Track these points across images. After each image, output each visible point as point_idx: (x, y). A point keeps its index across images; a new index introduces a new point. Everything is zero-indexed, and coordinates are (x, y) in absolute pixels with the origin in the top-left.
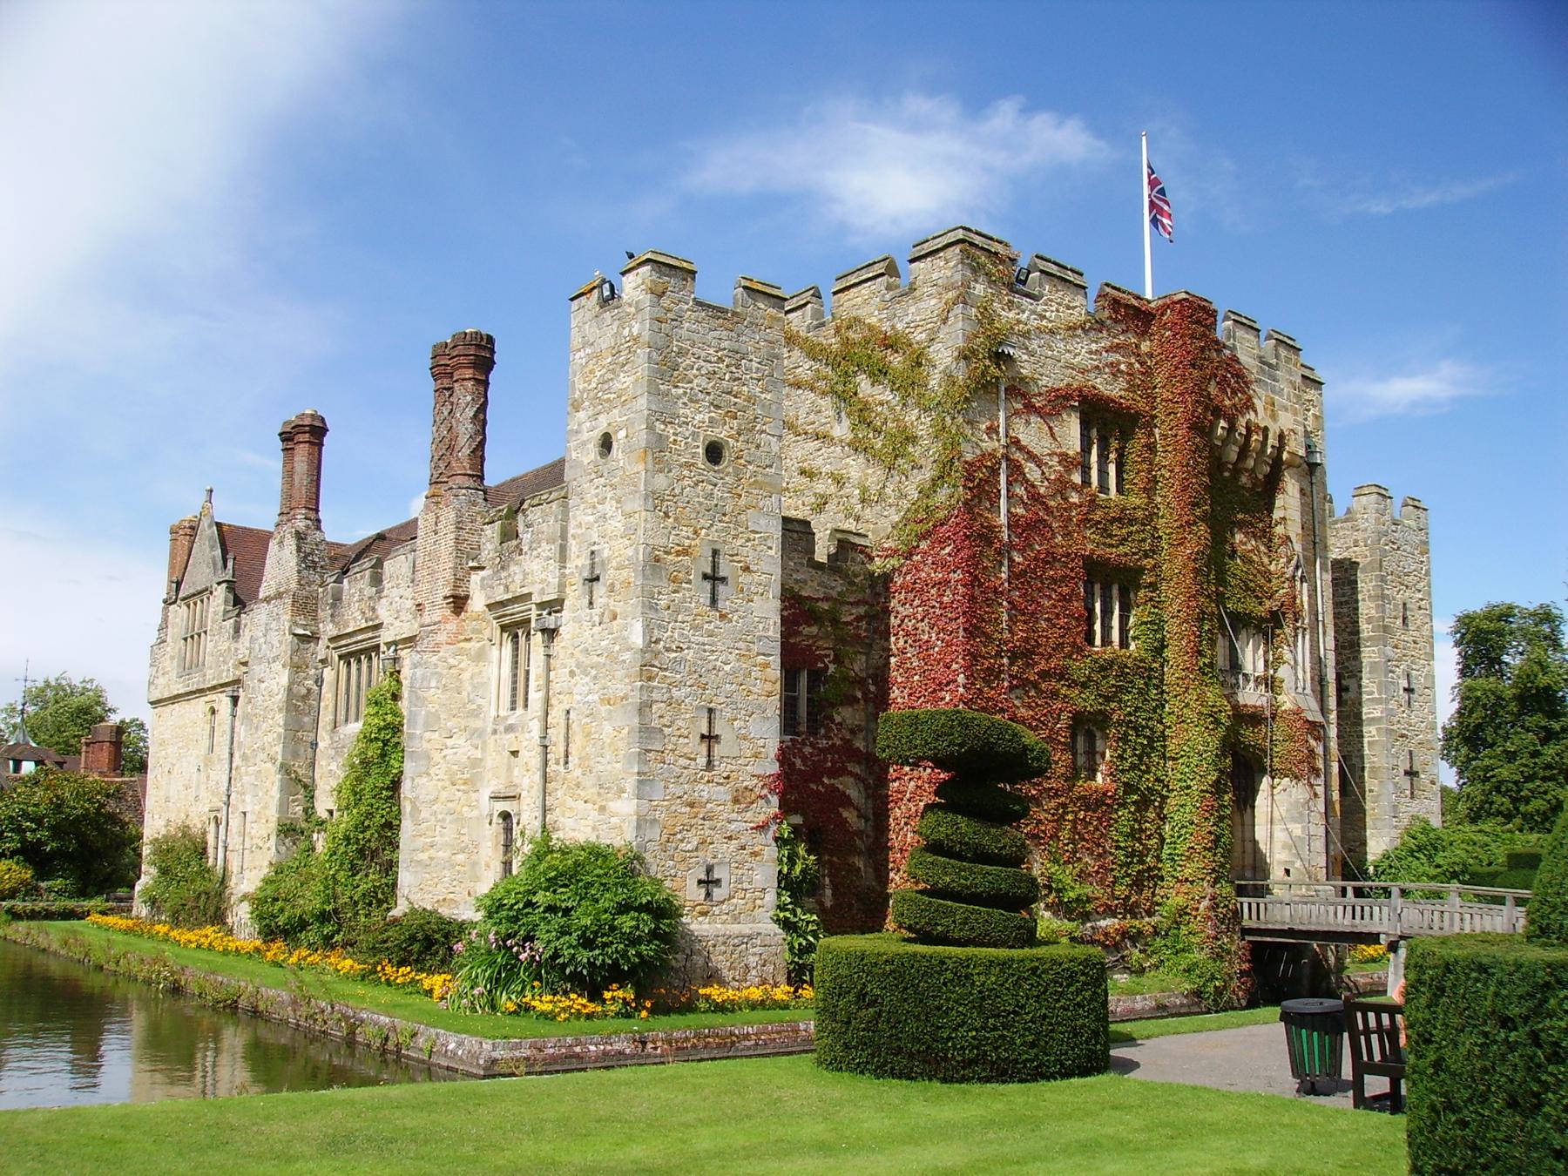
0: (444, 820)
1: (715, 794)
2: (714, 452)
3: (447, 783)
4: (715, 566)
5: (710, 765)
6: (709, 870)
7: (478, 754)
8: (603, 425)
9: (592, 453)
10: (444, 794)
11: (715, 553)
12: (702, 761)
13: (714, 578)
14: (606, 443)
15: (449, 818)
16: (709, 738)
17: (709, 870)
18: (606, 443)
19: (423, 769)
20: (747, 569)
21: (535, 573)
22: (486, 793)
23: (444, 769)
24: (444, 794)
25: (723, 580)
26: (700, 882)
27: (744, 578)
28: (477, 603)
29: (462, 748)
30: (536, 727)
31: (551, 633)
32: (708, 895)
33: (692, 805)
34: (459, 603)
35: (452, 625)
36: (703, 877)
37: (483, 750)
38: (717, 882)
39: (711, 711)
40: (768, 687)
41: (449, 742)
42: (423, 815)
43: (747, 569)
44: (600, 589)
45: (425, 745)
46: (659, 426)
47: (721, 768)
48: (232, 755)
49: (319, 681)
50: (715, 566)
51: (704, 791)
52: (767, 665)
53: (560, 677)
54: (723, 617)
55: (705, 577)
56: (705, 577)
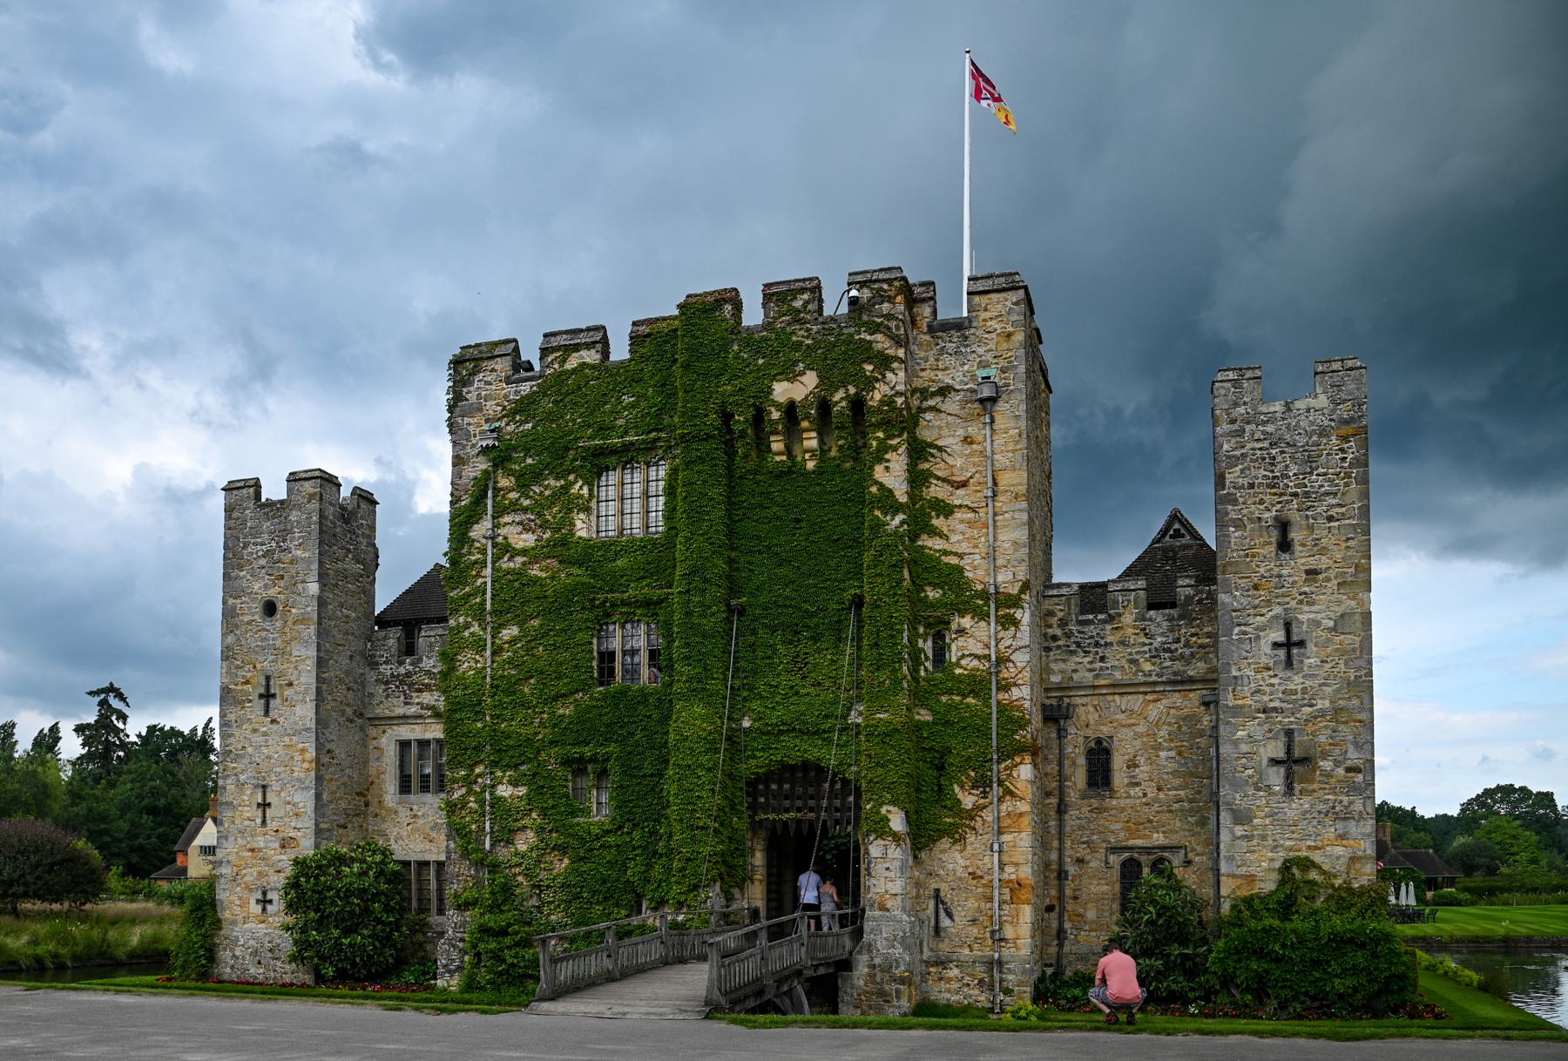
1: (267, 842)
4: (268, 687)
5: (264, 822)
6: (264, 893)
11: (268, 678)
12: (259, 821)
13: (267, 696)
16: (265, 805)
17: (264, 893)
20: (290, 684)
25: (274, 696)
26: (258, 901)
27: (288, 692)
32: (264, 909)
33: (252, 850)
36: (260, 897)
38: (270, 902)
39: (264, 787)
40: (306, 765)
43: (290, 684)
46: (231, 601)
47: (272, 825)
50: (268, 687)
51: (260, 842)
52: (303, 750)
54: (273, 721)
55: (261, 696)
56: (261, 696)
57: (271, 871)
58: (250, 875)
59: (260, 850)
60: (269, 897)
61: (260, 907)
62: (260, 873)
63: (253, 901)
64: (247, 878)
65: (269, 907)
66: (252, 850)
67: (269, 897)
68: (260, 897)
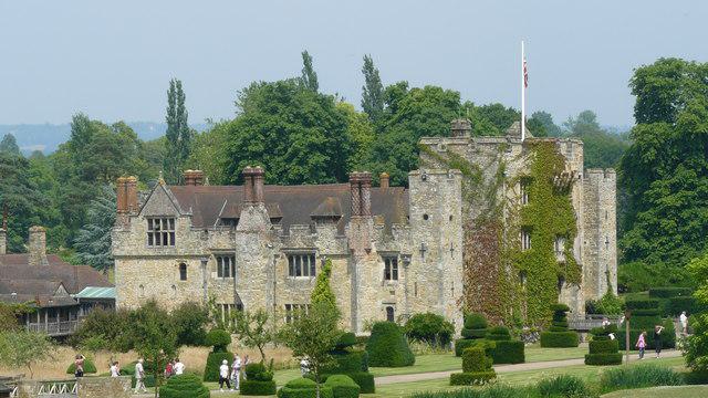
2: (451, 218)
8: (424, 212)
9: (420, 219)
14: (426, 217)
18: (426, 217)
21: (400, 246)
22: (379, 303)
28: (374, 250)
29: (372, 290)
30: (402, 287)
31: (407, 264)
34: (368, 251)
35: (367, 257)
44: (426, 255)
48: (205, 282)
49: (275, 262)
53: (411, 274)
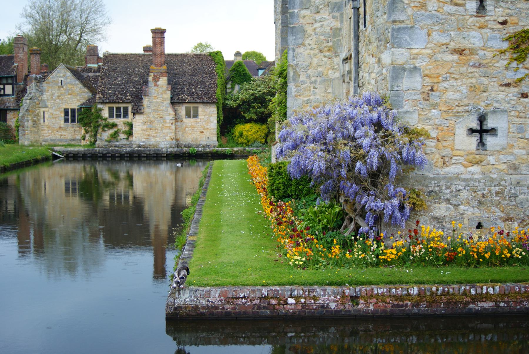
0: (315, 82)
3: (317, 51)
6: (482, 119)
7: (337, 24)
10: (315, 61)
15: (319, 79)
17: (482, 119)
19: (300, 41)
23: (314, 39)
24: (315, 61)
32: (482, 143)
33: (460, 52)
36: (475, 125)
37: (342, 21)
38: (493, 131)
41: (318, 17)
42: (302, 78)
45: (302, 21)
51: (474, 39)
57: (493, 86)
58: (455, 91)
59: (473, 52)
60: (490, 124)
61: (474, 139)
62: (473, 88)
63: (461, 132)
64: (451, 95)
65: (489, 140)
66: (460, 52)
67: (490, 124)
68: (475, 125)
